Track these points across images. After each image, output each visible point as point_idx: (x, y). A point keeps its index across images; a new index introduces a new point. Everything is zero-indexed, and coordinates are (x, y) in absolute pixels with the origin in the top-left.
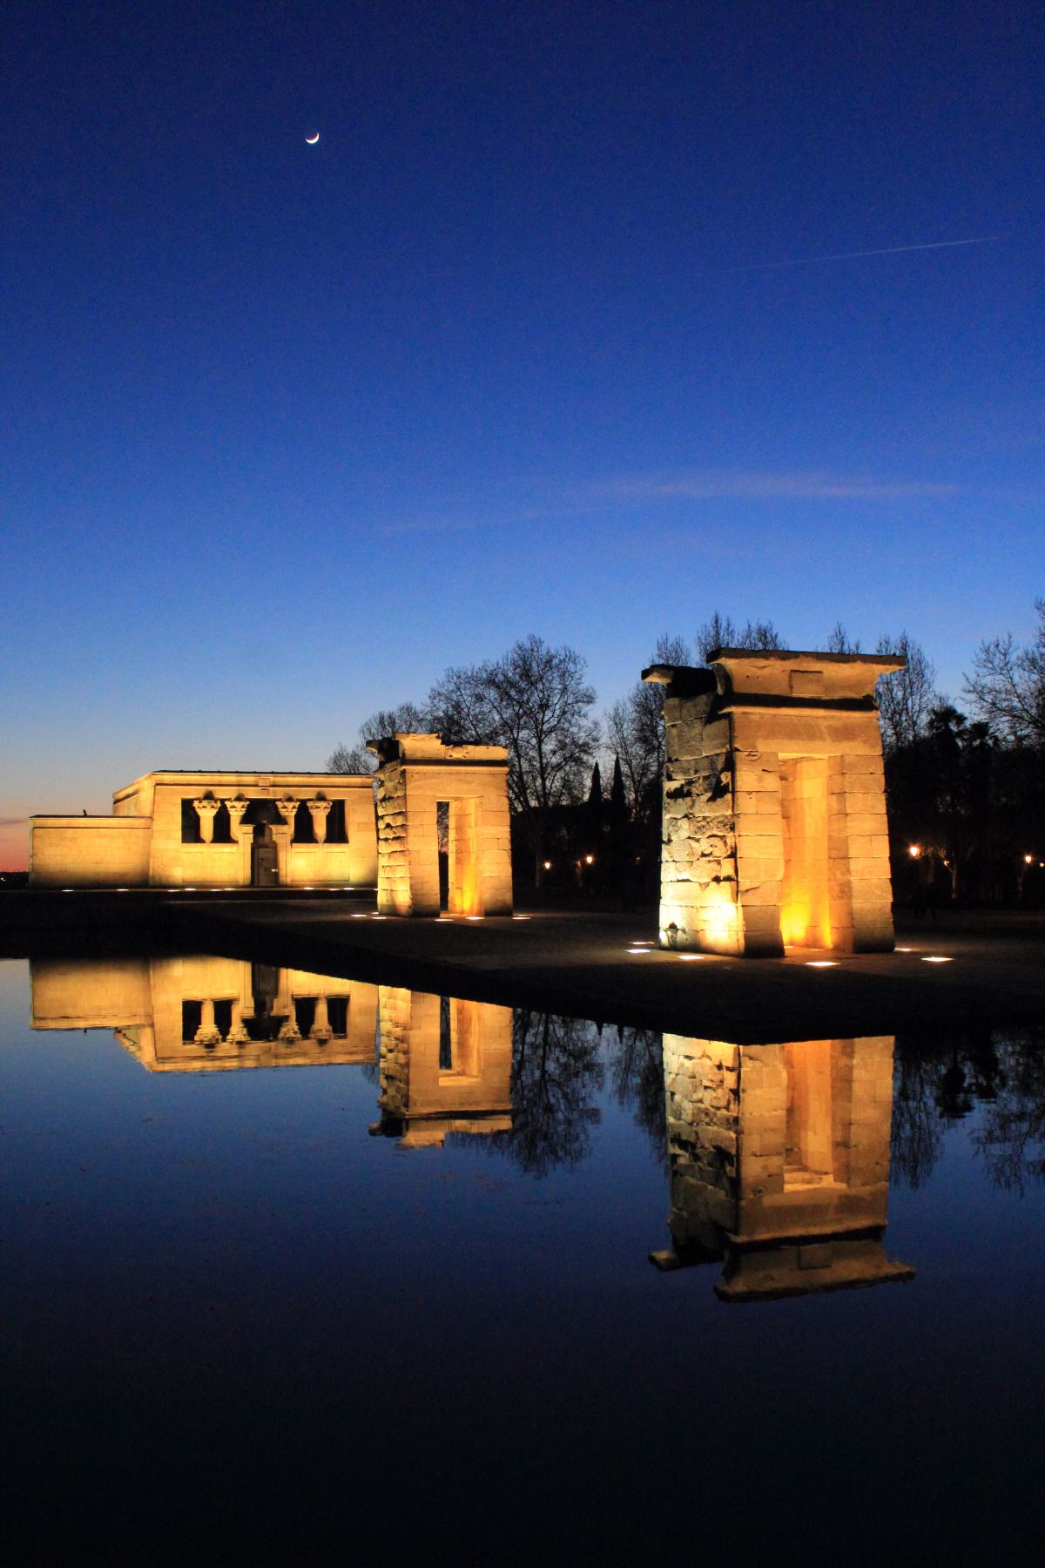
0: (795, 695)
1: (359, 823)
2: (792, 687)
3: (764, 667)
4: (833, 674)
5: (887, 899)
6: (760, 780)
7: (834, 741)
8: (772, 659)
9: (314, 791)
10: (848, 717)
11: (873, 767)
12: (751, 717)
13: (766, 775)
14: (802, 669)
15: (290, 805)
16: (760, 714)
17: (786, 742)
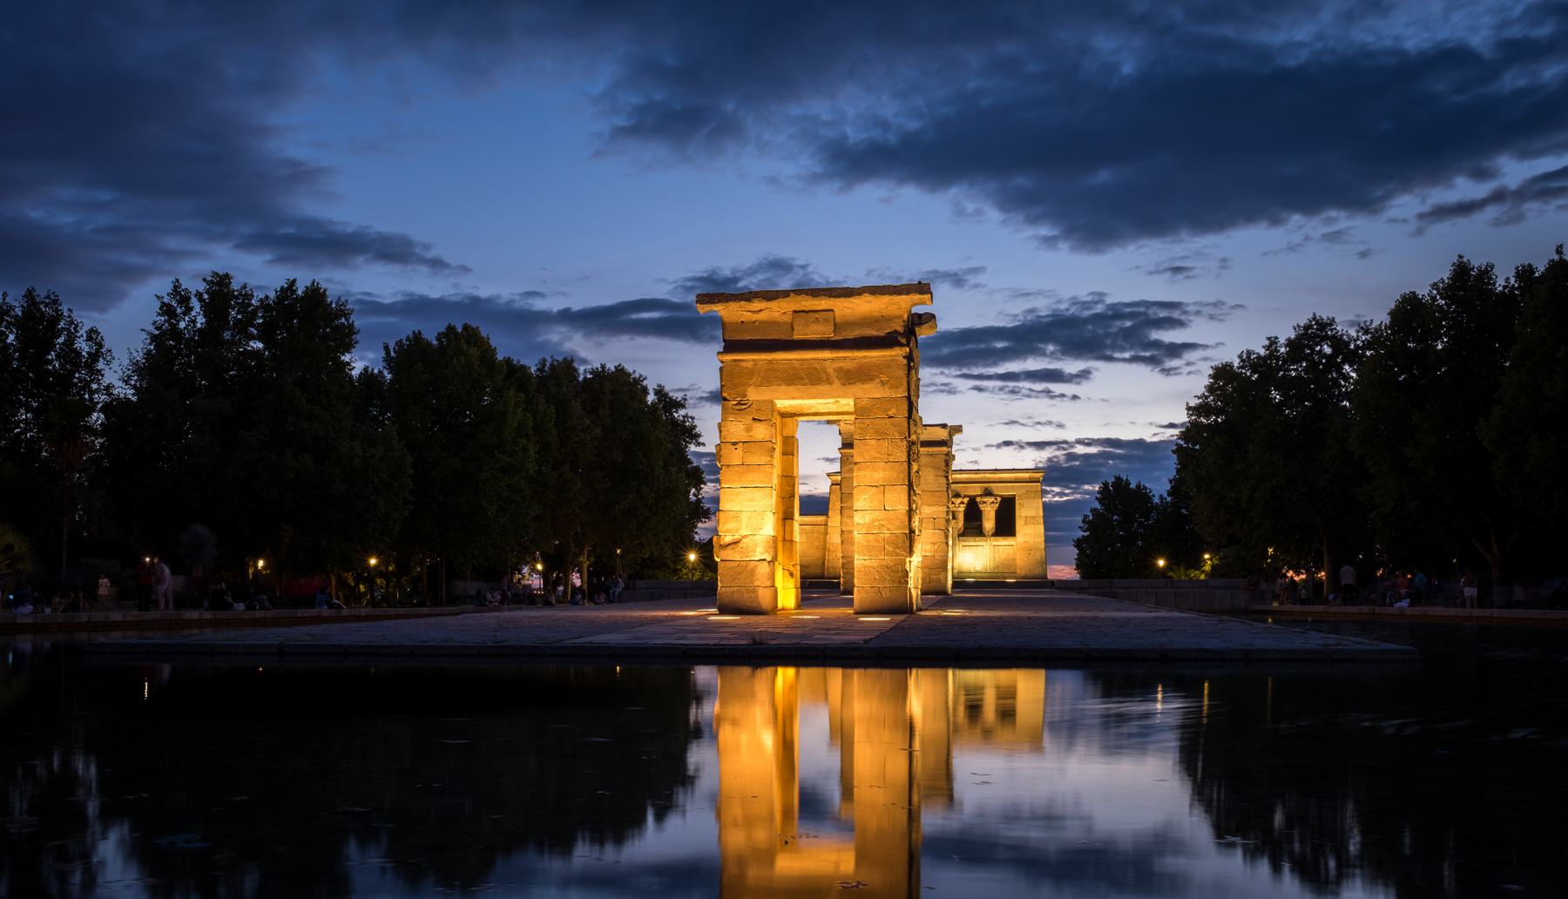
0: (796, 337)
1: (1026, 517)
2: (793, 329)
3: (761, 310)
4: (847, 312)
5: (902, 555)
6: (749, 430)
7: (845, 385)
8: (756, 301)
9: (981, 487)
10: (865, 357)
11: (894, 411)
12: (743, 364)
13: (757, 424)
14: (806, 309)
15: (959, 500)
16: (754, 360)
17: (784, 388)
